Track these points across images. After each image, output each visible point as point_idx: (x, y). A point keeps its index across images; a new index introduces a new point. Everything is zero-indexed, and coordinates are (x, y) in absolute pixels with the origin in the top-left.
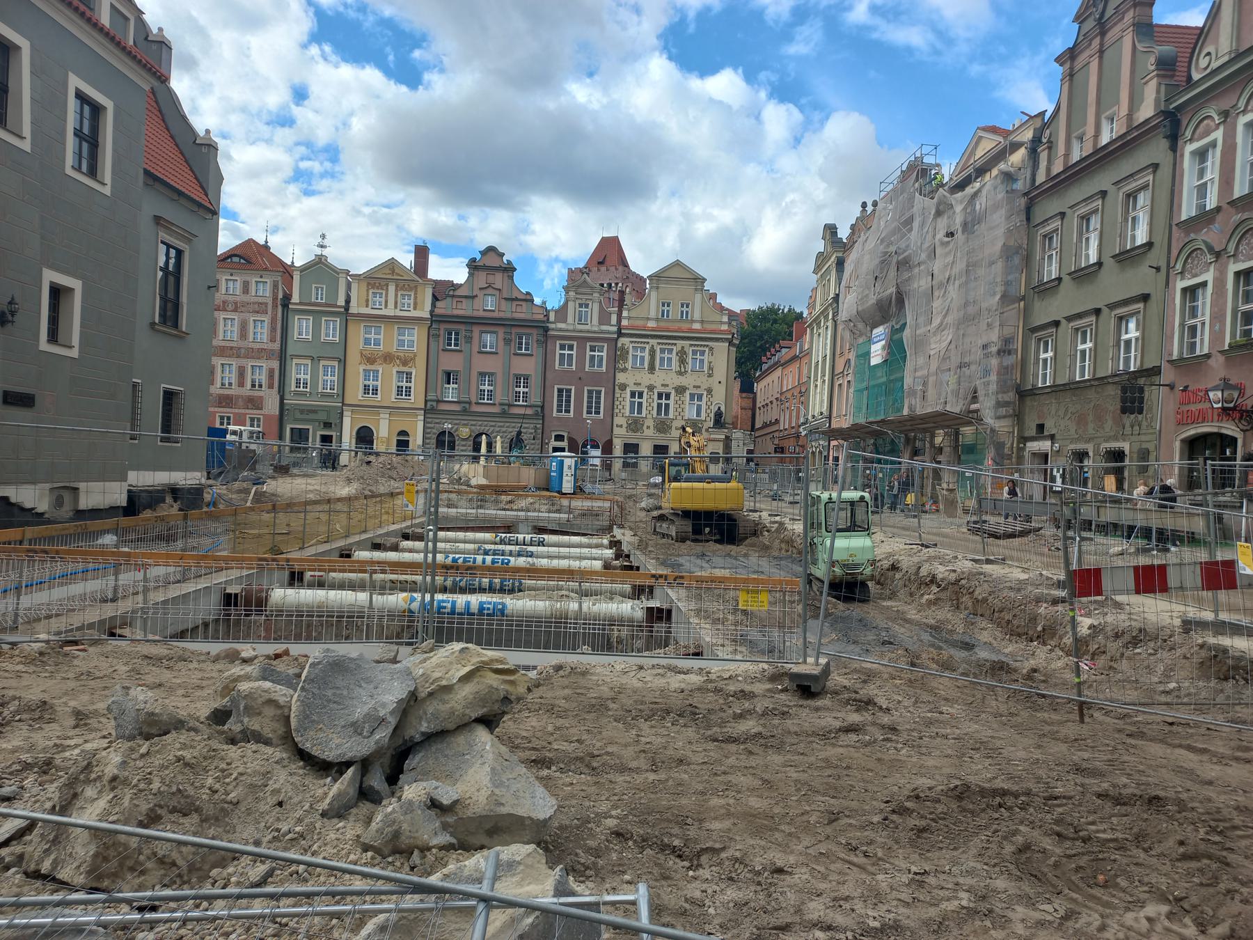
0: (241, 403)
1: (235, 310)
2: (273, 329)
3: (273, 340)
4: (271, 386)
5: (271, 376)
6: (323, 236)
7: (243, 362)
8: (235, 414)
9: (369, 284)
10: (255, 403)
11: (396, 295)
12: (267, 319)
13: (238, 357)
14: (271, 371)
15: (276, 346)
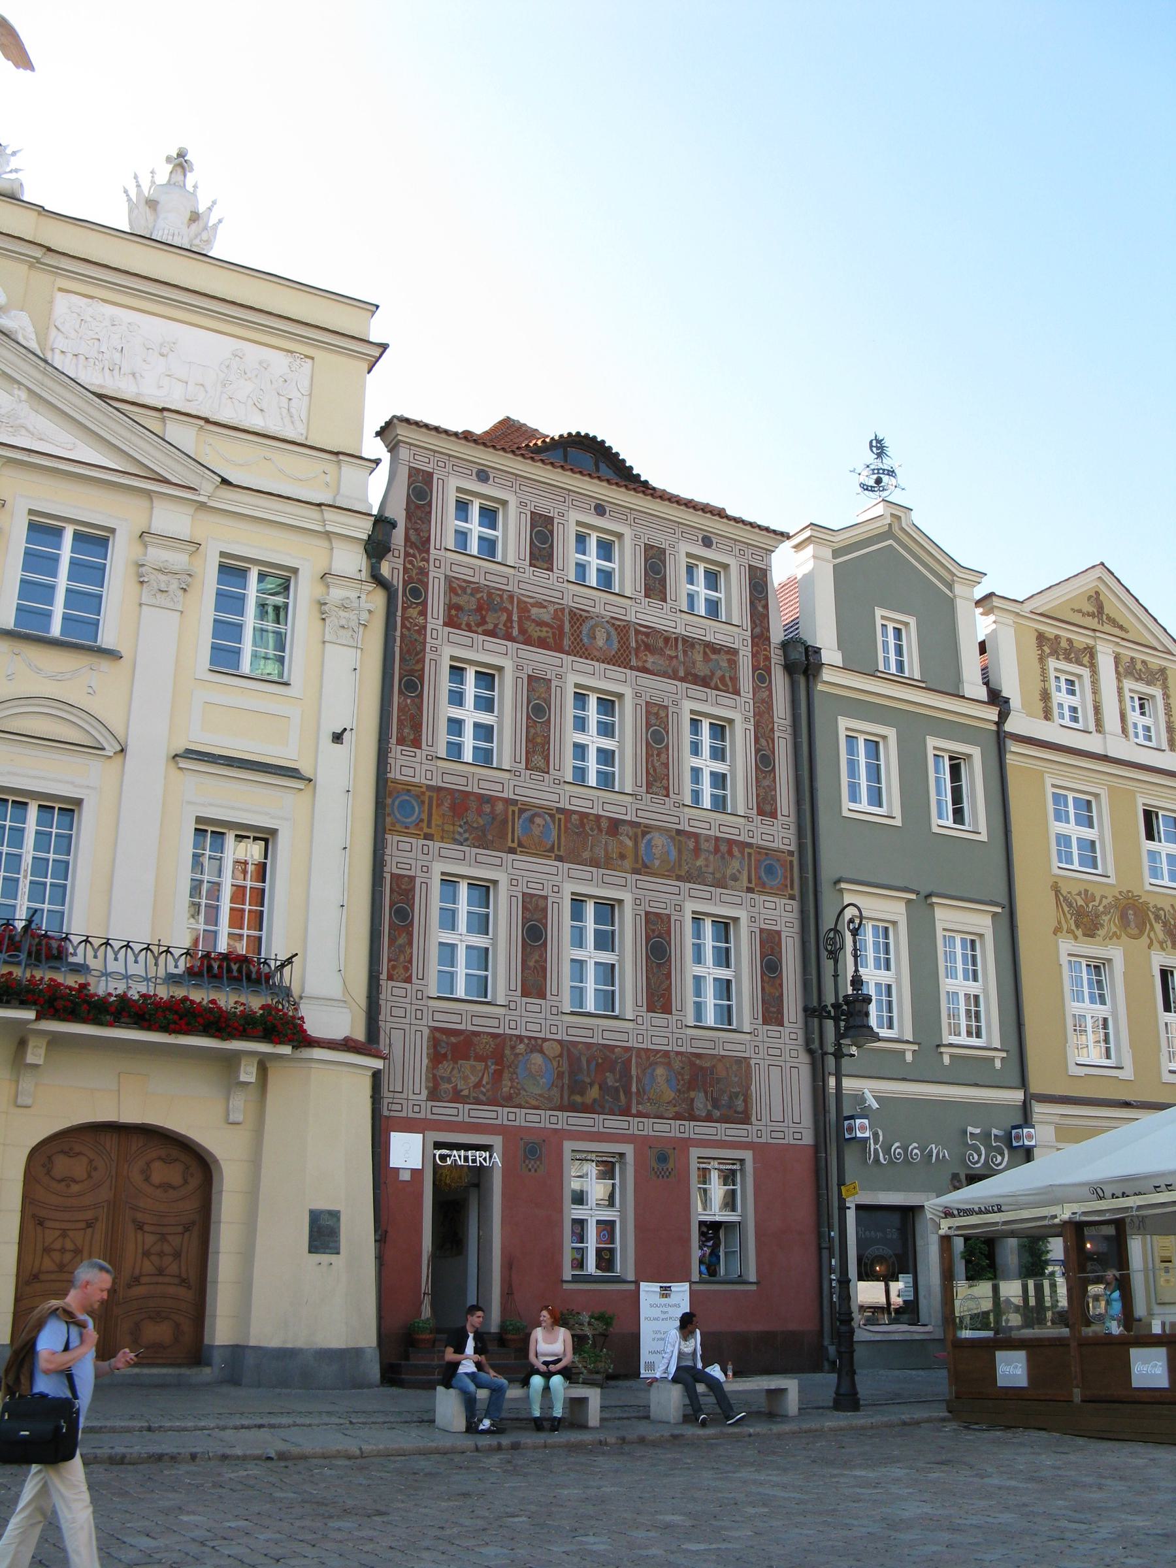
0: (661, 1081)
1: (620, 659)
2: (764, 761)
3: (766, 807)
4: (772, 1013)
5: (770, 967)
6: (879, 447)
7: (662, 893)
8: (643, 1143)
9: (1041, 637)
10: (712, 1087)
11: (1120, 690)
12: (737, 712)
13: (642, 868)
14: (769, 944)
15: (779, 835)
